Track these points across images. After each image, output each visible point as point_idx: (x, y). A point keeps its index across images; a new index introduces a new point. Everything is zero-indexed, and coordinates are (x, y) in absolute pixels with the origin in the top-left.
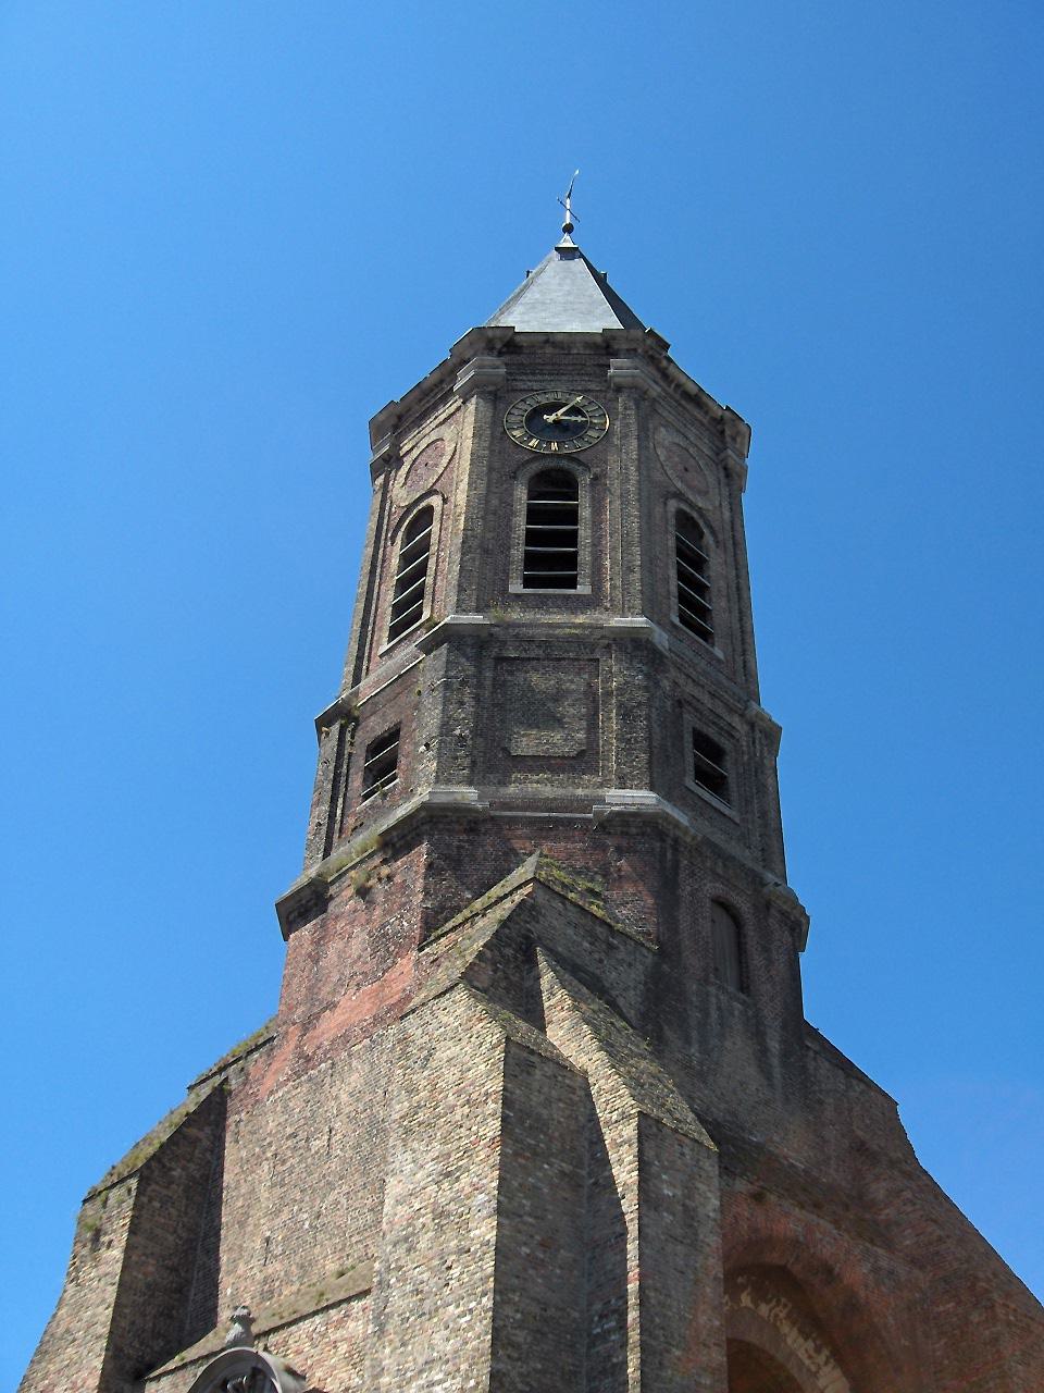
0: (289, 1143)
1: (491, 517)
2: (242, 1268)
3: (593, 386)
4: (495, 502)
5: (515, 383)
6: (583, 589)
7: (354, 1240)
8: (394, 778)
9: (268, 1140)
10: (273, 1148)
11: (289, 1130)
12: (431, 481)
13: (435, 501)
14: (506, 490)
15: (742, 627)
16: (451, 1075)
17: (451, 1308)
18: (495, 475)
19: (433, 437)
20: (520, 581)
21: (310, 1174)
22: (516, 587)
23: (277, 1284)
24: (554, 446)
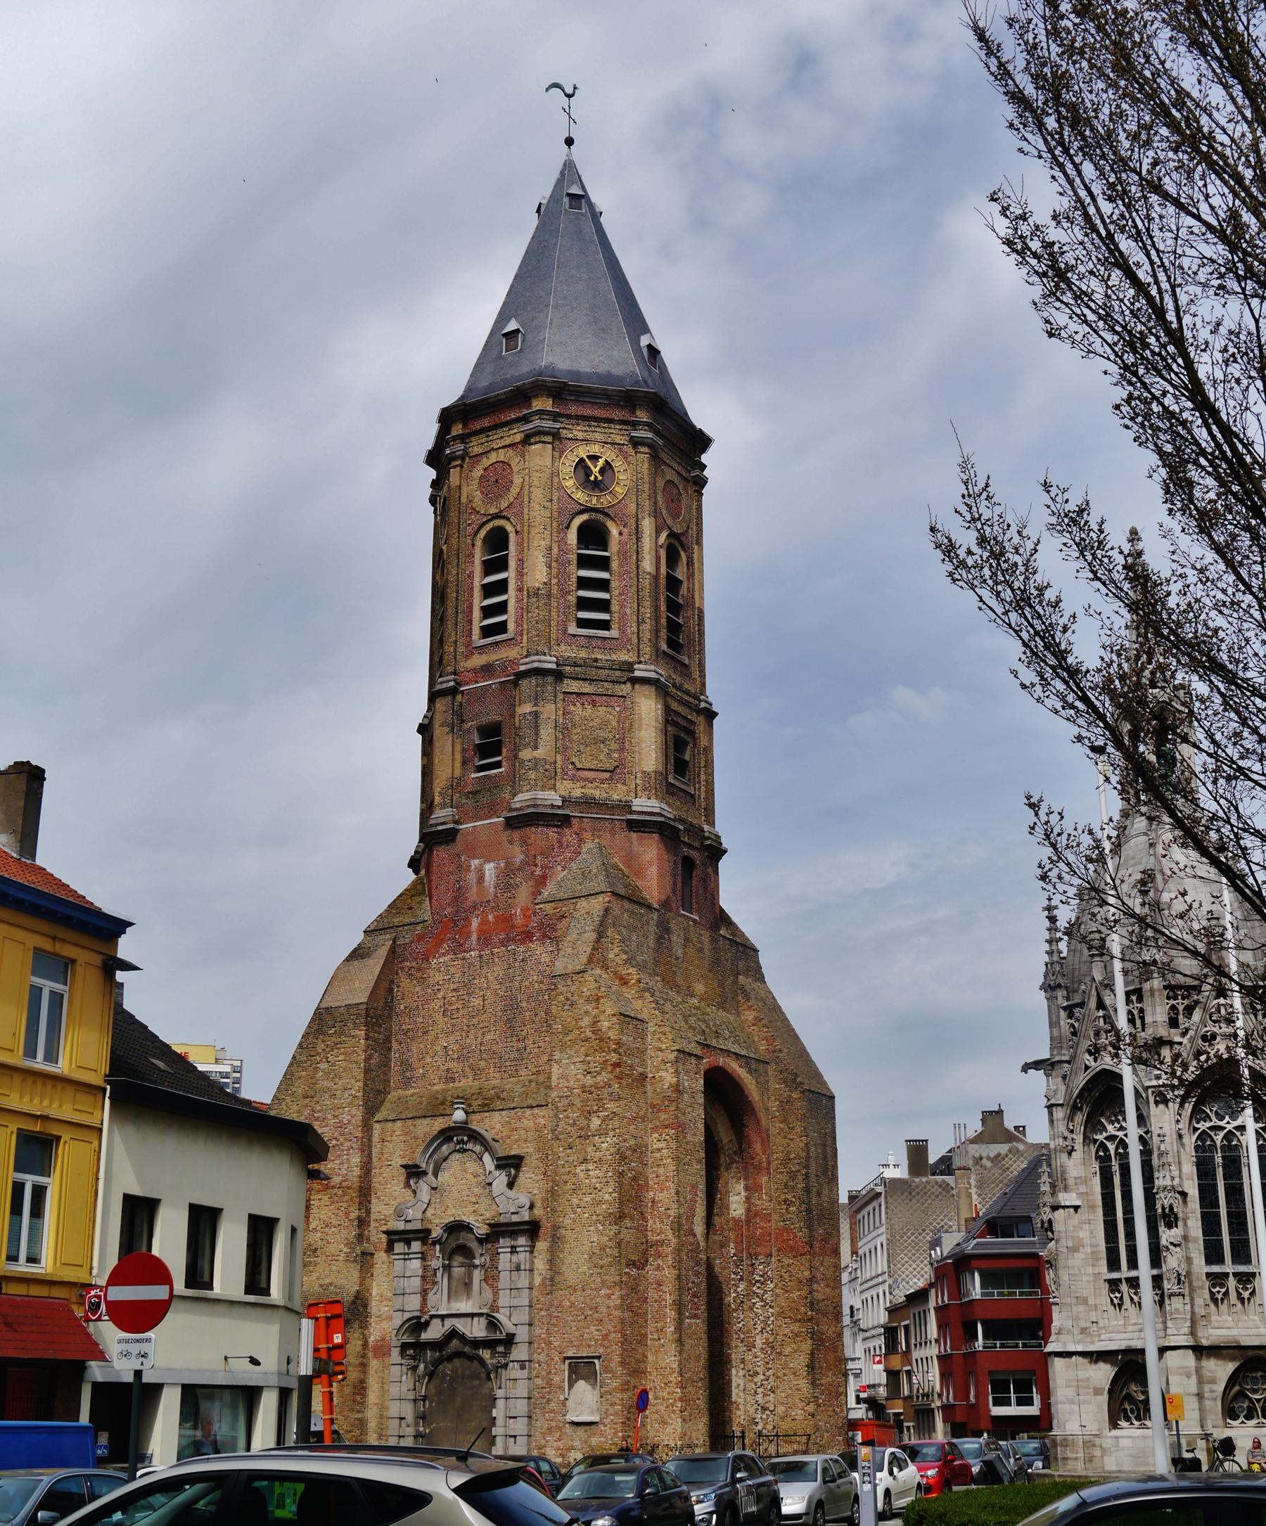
0: (454, 994)
1: (554, 564)
2: (429, 1060)
3: (618, 439)
4: (555, 550)
5: (564, 431)
6: (614, 633)
7: (507, 1064)
8: (498, 765)
9: (438, 987)
10: (442, 993)
11: (452, 987)
12: (504, 504)
13: (509, 528)
14: (563, 538)
15: (699, 630)
16: (586, 1022)
17: (597, 1138)
18: (555, 524)
19: (502, 455)
20: (575, 624)
21: (473, 1017)
22: (573, 629)
23: (457, 1075)
24: (594, 501)
